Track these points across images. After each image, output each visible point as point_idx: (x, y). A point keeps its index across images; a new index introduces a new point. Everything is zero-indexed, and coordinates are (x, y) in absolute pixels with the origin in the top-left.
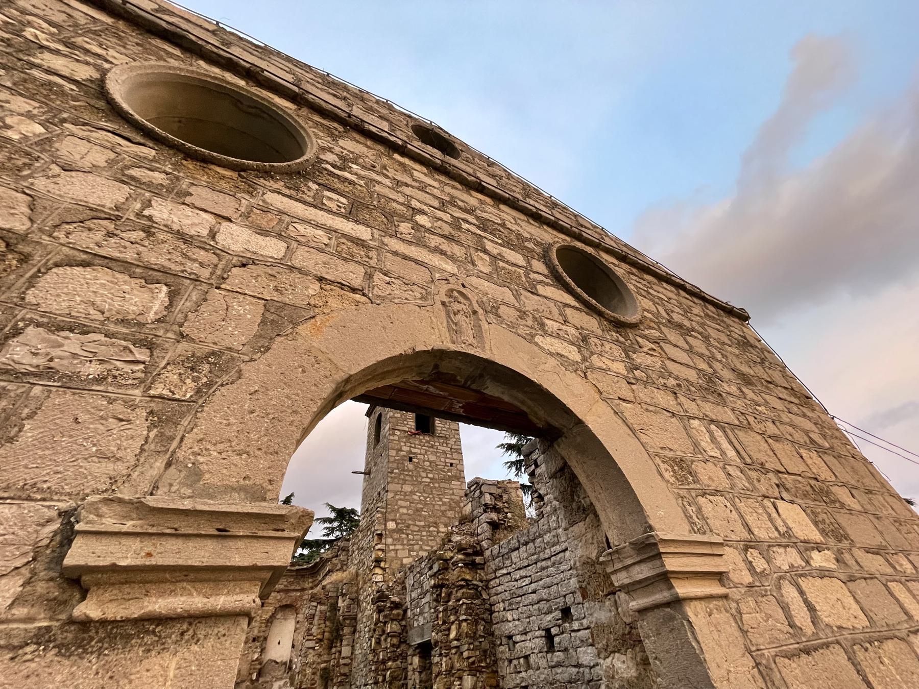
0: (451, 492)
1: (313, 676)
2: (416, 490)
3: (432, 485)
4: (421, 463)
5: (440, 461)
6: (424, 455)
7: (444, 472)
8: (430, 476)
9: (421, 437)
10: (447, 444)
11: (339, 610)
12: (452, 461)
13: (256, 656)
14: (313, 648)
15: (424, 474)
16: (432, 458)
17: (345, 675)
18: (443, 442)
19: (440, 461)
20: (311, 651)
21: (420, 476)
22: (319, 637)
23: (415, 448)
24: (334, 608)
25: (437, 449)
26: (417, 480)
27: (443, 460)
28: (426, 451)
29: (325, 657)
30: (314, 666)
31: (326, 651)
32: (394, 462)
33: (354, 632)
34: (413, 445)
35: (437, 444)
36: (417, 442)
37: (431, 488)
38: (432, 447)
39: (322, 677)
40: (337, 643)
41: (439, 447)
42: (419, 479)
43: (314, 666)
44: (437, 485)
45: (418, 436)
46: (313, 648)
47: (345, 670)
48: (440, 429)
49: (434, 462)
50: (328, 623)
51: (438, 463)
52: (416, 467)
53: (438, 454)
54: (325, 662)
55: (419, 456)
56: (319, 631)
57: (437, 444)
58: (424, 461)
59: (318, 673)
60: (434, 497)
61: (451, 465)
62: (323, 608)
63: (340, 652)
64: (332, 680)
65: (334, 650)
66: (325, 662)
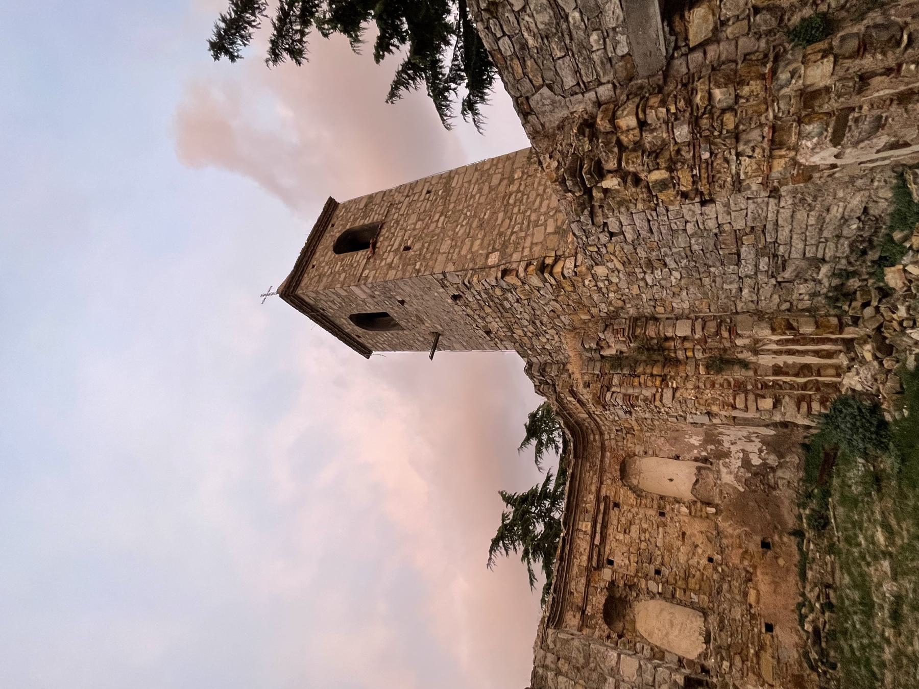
0: (466, 185)
1: (717, 386)
2: (450, 233)
4: (415, 233)
7: (436, 199)
10: (400, 203)
11: (621, 352)
12: (424, 192)
13: (684, 510)
14: (675, 390)
17: (719, 326)
20: (678, 395)
22: (658, 383)
23: (393, 245)
24: (618, 361)
27: (418, 205)
29: (690, 369)
30: (702, 385)
31: (681, 368)
32: (404, 271)
33: (656, 320)
34: (389, 249)
35: (396, 216)
36: (386, 244)
38: (397, 222)
39: (719, 371)
40: (669, 350)
41: (401, 212)
43: (702, 385)
45: (378, 244)
46: (675, 390)
47: (712, 327)
50: (640, 370)
54: (697, 366)
56: (649, 383)
57: (396, 216)
59: (713, 377)
61: (428, 192)
62: (615, 381)
63: (685, 339)
64: (725, 350)
65: (680, 355)
66: (697, 366)
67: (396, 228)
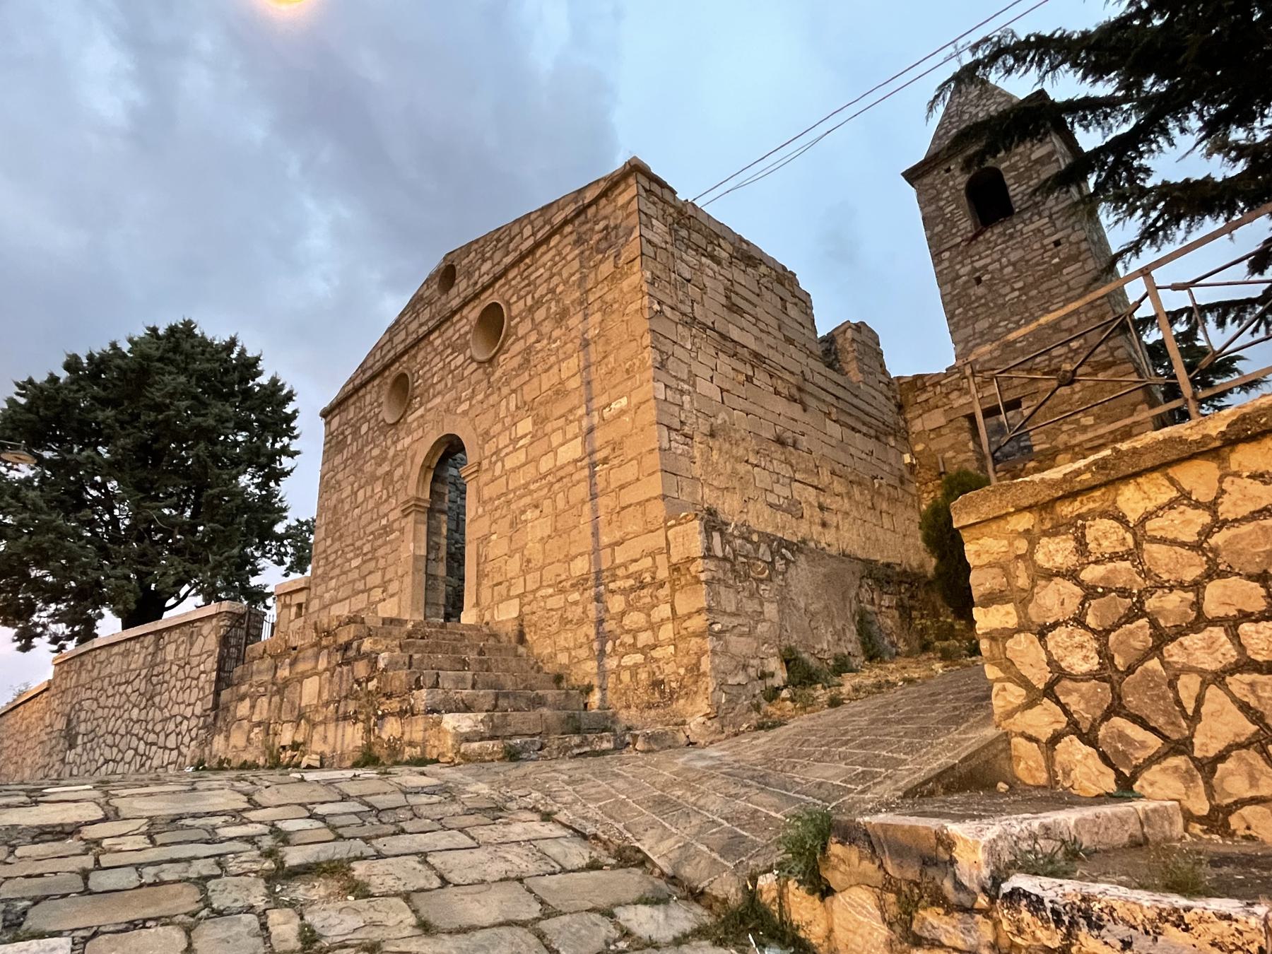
3: (1024, 298)
5: (1033, 250)
6: (999, 260)
8: (1020, 284)
9: (988, 235)
15: (1008, 289)
16: (1014, 256)
18: (1030, 218)
19: (1033, 250)
21: (1000, 295)
25: (1022, 234)
26: (996, 305)
28: (1002, 251)
37: (1025, 302)
42: (1000, 301)
44: (1034, 292)
48: (1019, 197)
49: (1022, 259)
51: (1027, 257)
52: (990, 287)
53: (1026, 242)
55: (990, 268)
58: (1002, 268)
60: (1032, 314)
67: (1004, 242)
